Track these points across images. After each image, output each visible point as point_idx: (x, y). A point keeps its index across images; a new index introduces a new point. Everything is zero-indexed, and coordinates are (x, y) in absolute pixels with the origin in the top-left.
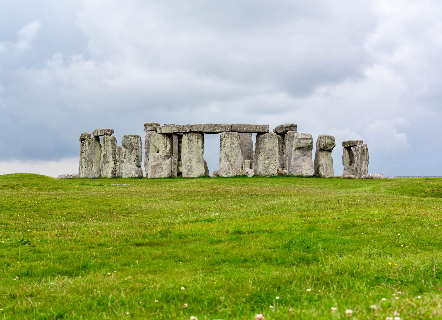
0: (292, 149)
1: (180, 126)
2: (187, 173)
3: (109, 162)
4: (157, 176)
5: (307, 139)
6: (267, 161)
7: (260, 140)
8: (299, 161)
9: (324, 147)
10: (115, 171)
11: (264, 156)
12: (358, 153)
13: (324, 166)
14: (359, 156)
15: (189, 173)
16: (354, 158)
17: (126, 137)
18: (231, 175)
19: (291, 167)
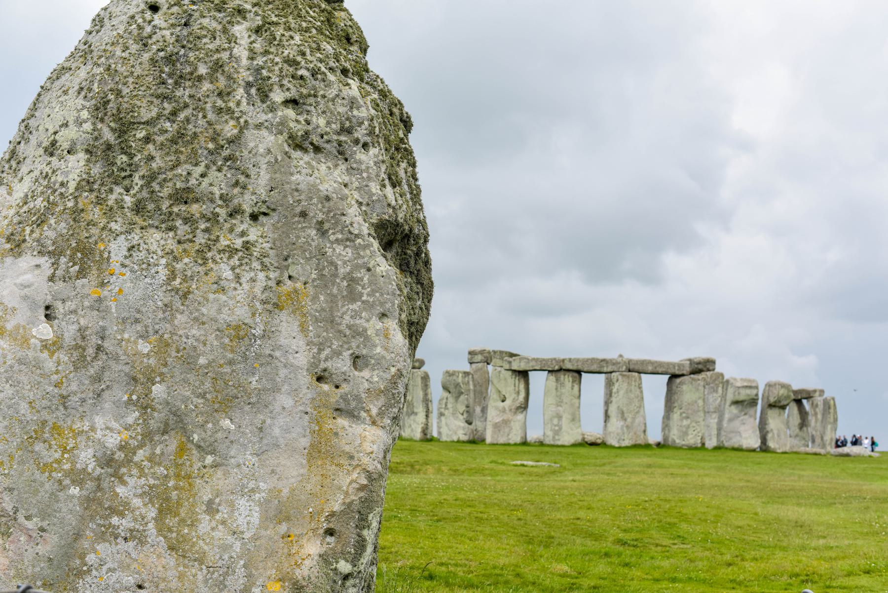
0: (725, 404)
1: (544, 360)
2: (554, 437)
3: (416, 414)
4: (502, 440)
5: (750, 387)
6: (685, 422)
7: (674, 388)
8: (737, 423)
9: (775, 402)
10: (427, 428)
11: (681, 414)
12: (817, 410)
13: (775, 432)
14: (820, 416)
15: (557, 437)
16: (810, 418)
17: (450, 374)
18: (627, 443)
19: (723, 433)
